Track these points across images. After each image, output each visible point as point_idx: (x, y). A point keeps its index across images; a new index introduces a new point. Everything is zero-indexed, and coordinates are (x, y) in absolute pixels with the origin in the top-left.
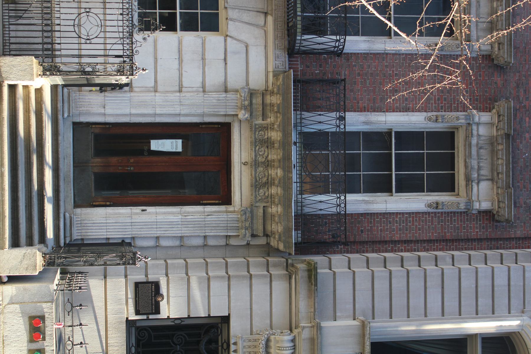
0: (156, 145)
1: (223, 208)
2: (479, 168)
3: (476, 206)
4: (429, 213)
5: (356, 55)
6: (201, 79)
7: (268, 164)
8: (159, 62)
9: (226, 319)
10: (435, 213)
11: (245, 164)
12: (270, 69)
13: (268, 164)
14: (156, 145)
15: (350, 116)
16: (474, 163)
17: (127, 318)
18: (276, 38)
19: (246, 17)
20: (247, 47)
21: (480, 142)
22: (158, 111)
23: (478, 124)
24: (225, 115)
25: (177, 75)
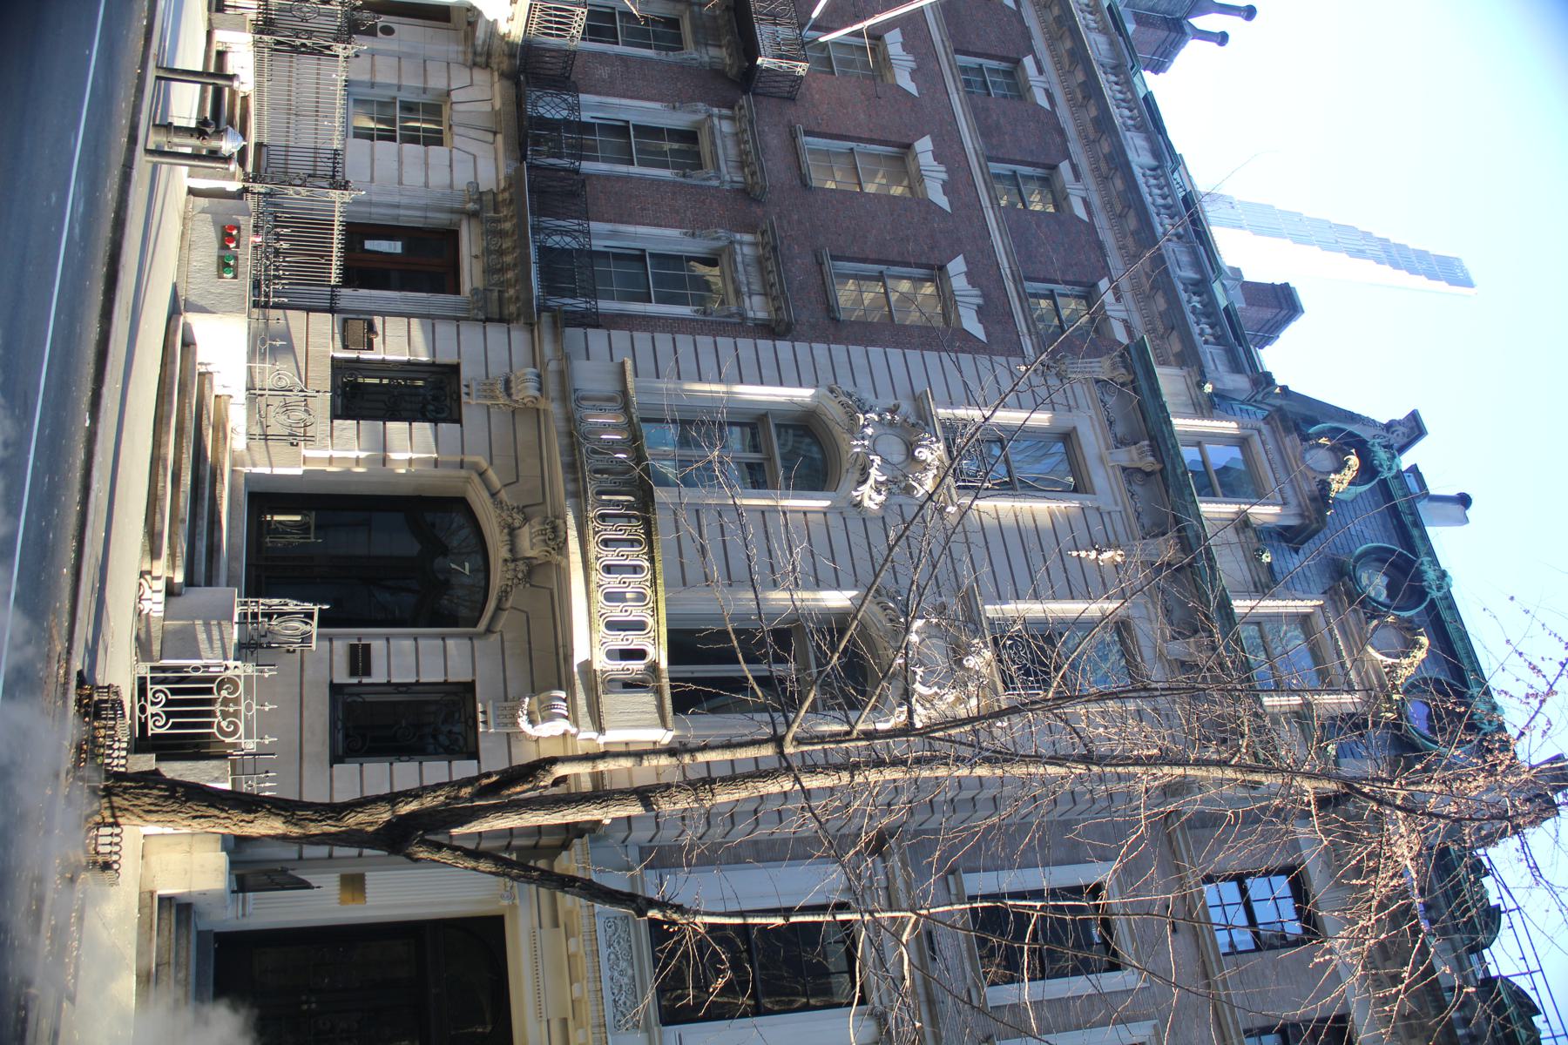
0: (370, 245)
1: (451, 298)
2: (749, 284)
3: (751, 314)
4: (697, 320)
5: (598, 177)
6: (423, 180)
7: (501, 252)
8: (376, 162)
9: (455, 369)
10: (704, 321)
11: (476, 257)
12: (502, 177)
13: (501, 252)
14: (370, 245)
15: (595, 226)
16: (742, 278)
17: (331, 682)
18: (506, 150)
19: (472, 133)
20: (475, 157)
21: (747, 260)
22: (375, 198)
23: (741, 243)
24: (452, 211)
25: (396, 173)
